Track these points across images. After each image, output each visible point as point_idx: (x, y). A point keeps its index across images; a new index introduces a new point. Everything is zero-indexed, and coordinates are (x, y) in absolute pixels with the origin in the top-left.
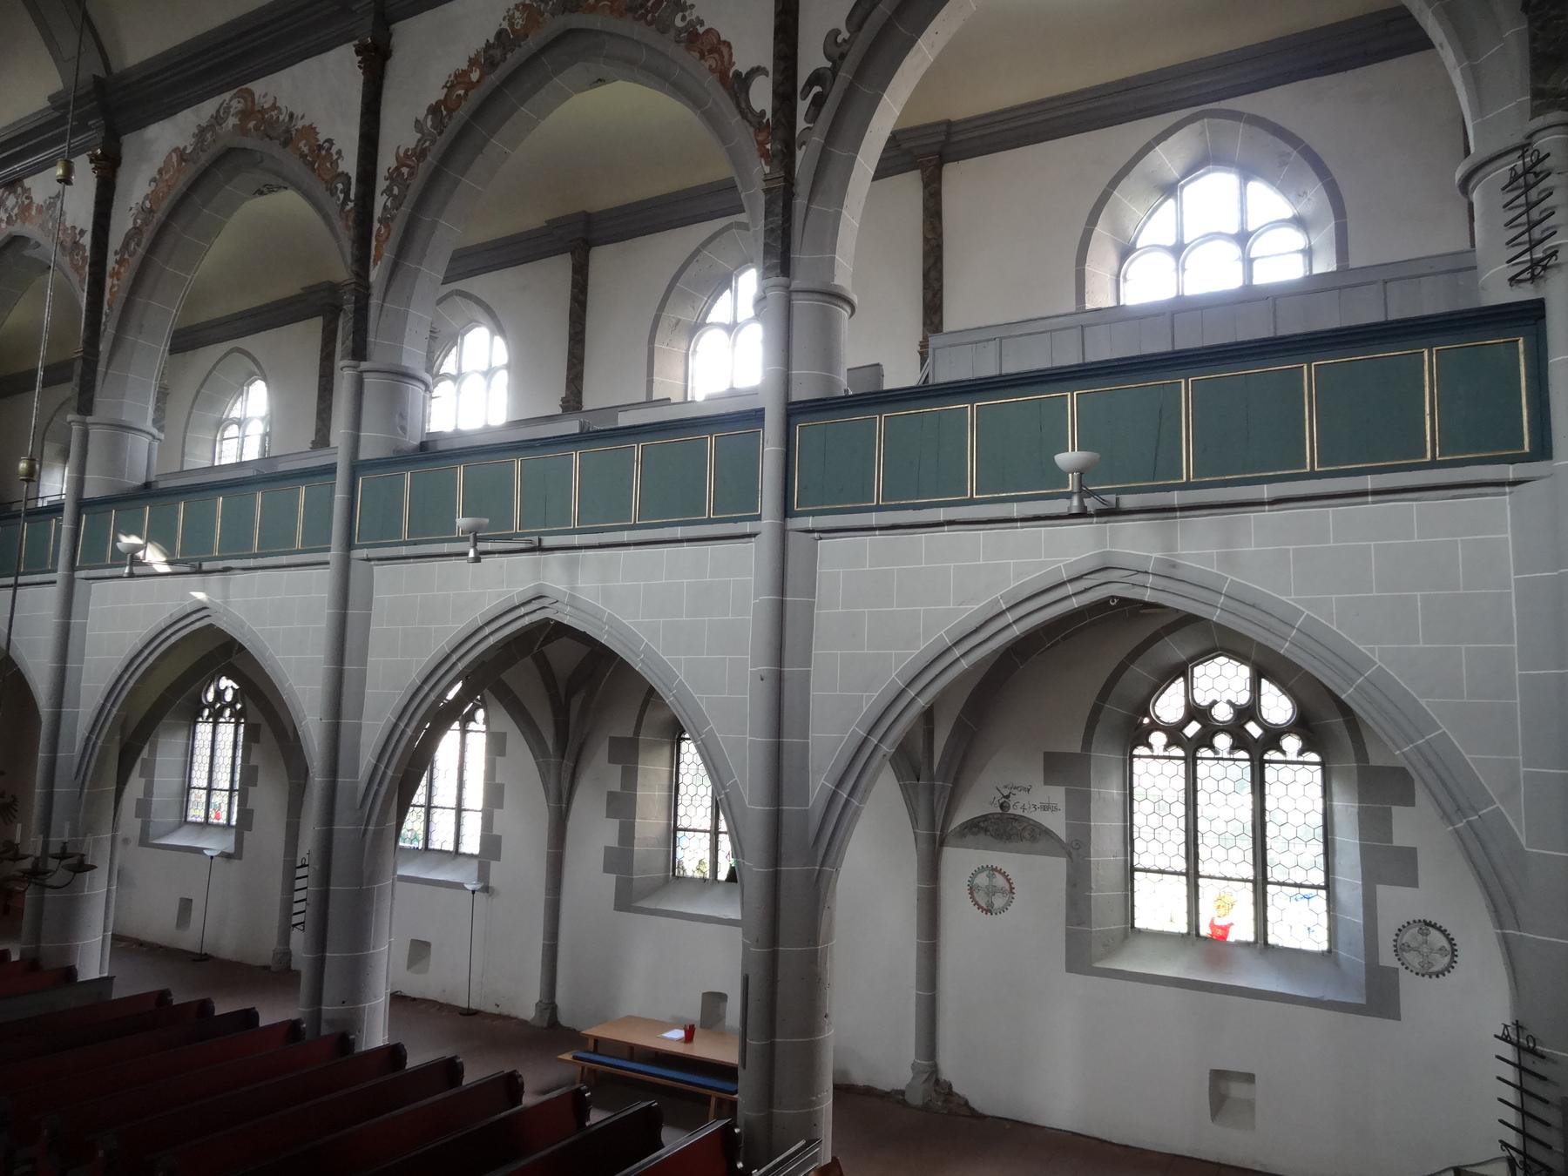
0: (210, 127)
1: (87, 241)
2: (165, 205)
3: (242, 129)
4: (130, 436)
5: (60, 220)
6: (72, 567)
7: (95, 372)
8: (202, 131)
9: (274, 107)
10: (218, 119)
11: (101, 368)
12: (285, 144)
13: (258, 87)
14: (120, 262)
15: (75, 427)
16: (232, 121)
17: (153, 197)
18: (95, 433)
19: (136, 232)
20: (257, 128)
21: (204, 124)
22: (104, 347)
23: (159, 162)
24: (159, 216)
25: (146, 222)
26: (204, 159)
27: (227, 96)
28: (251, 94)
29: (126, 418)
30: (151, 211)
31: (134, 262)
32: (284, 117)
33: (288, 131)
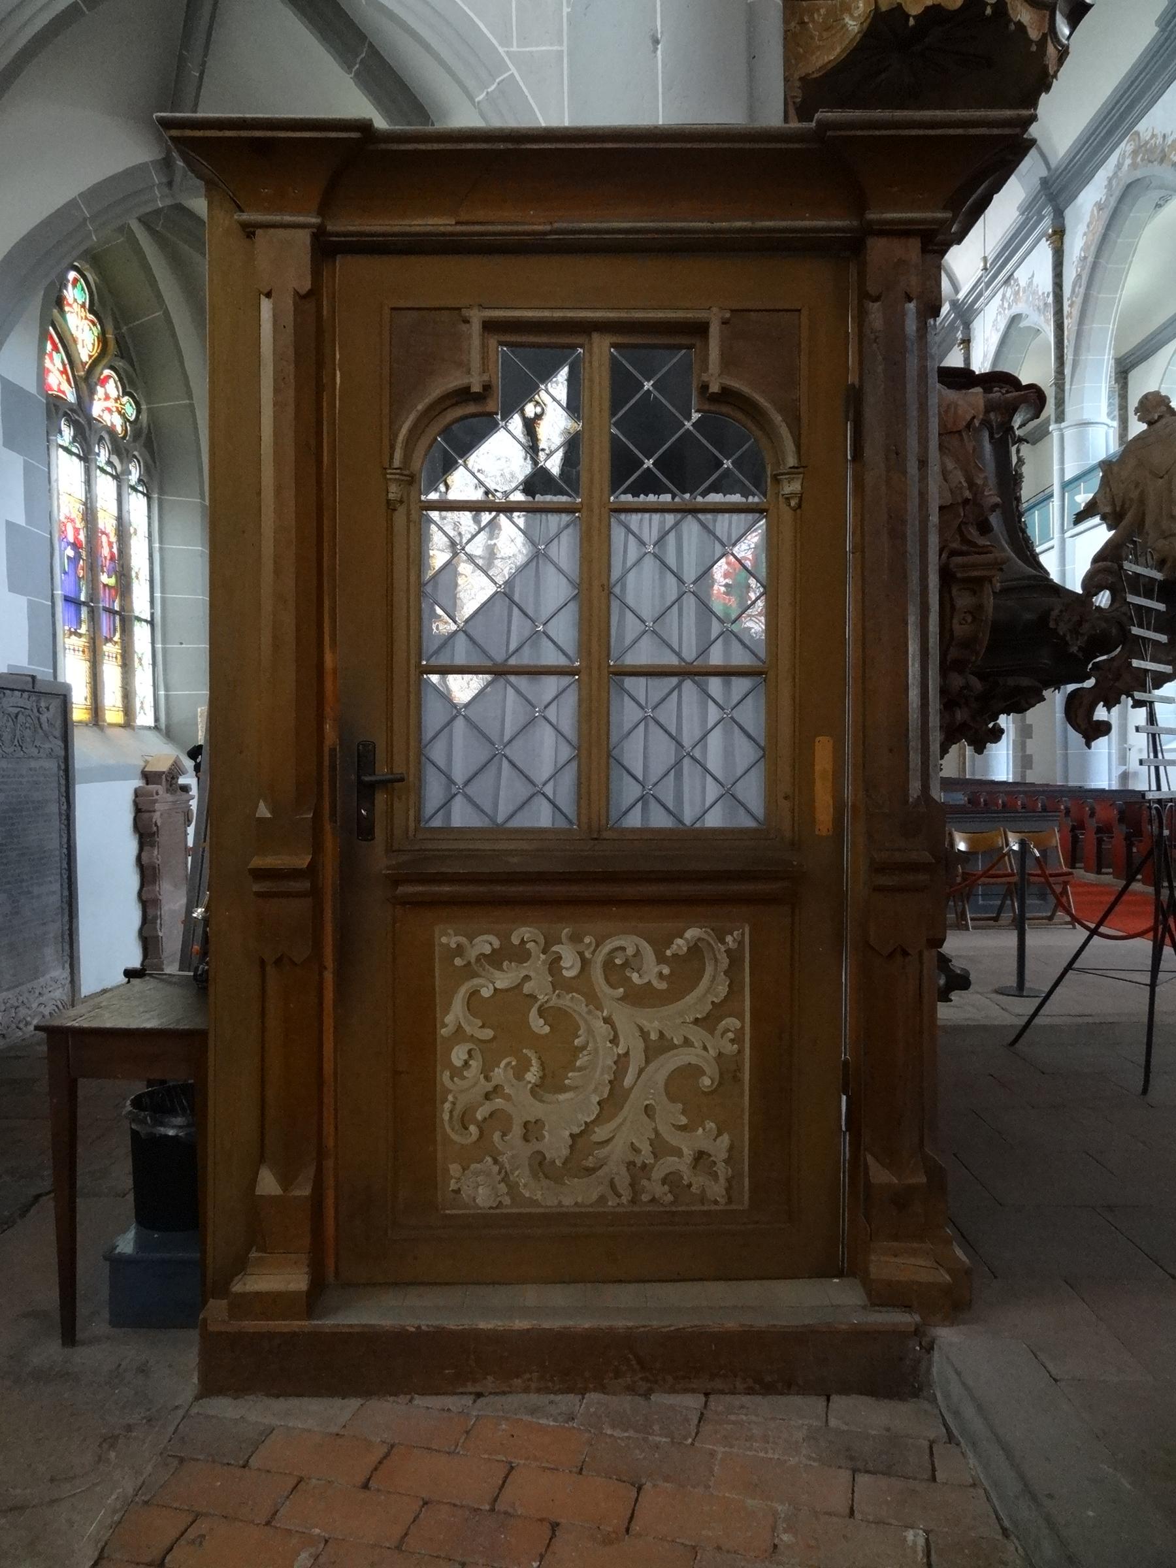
0: (1115, 173)
1: (1050, 300)
2: (1093, 249)
3: (1134, 166)
4: (1091, 430)
5: (1035, 293)
6: (1063, 531)
7: (1063, 391)
8: (1110, 180)
9: (1153, 136)
10: (1119, 166)
11: (1067, 387)
12: (1162, 161)
13: (1141, 127)
14: (1071, 306)
15: (1056, 434)
16: (1128, 161)
17: (1085, 248)
18: (1068, 433)
19: (1079, 276)
20: (1142, 160)
21: (1111, 175)
22: (1067, 371)
23: (1087, 219)
24: (1090, 259)
25: (1083, 268)
26: (1113, 202)
27: (1123, 145)
28: (1137, 133)
29: (1087, 416)
30: (1085, 258)
31: (1079, 300)
32: (1160, 140)
33: (1163, 150)
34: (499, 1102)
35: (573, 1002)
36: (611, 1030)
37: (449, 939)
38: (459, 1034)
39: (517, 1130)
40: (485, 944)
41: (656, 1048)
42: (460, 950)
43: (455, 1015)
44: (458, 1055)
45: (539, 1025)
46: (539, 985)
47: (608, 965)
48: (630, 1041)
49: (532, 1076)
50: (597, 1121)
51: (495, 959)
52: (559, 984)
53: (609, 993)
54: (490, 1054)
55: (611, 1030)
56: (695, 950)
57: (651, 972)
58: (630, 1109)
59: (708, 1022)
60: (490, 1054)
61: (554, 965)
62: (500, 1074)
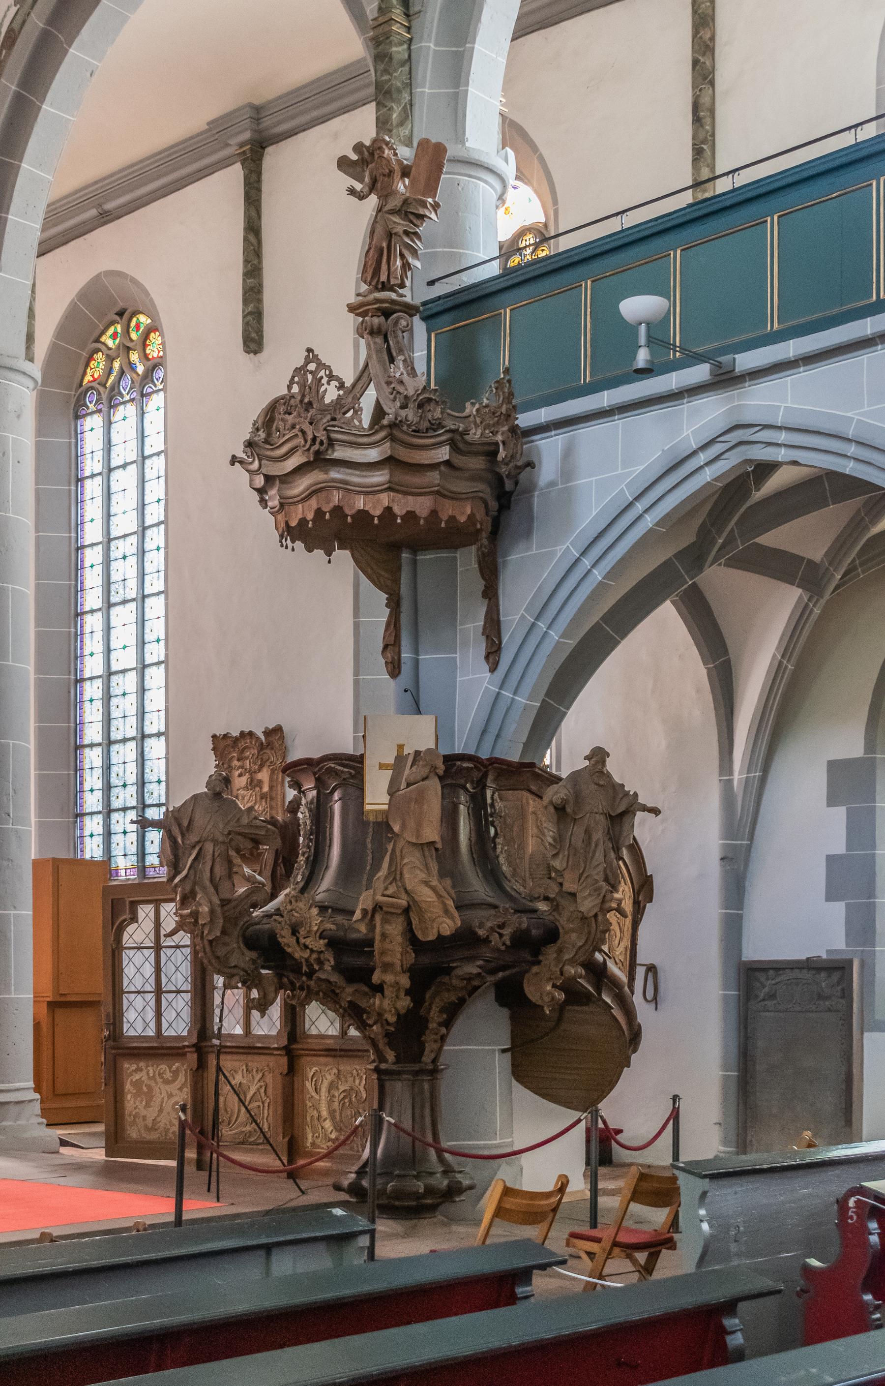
34: (137, 1110)
35: (152, 1083)
36: (161, 1091)
37: (126, 1065)
38: (129, 1092)
39: (141, 1119)
40: (134, 1067)
41: (170, 1096)
42: (128, 1069)
43: (128, 1087)
44: (129, 1097)
45: (145, 1089)
46: (145, 1078)
47: (159, 1074)
48: (164, 1094)
49: (144, 1103)
50: (158, 1116)
51: (136, 1071)
52: (149, 1078)
53: (159, 1080)
54: (136, 1096)
55: (161, 1091)
56: (178, 1070)
57: (168, 1075)
58: (165, 1113)
59: (180, 1089)
60: (136, 1096)
61: (148, 1073)
62: (137, 1102)
